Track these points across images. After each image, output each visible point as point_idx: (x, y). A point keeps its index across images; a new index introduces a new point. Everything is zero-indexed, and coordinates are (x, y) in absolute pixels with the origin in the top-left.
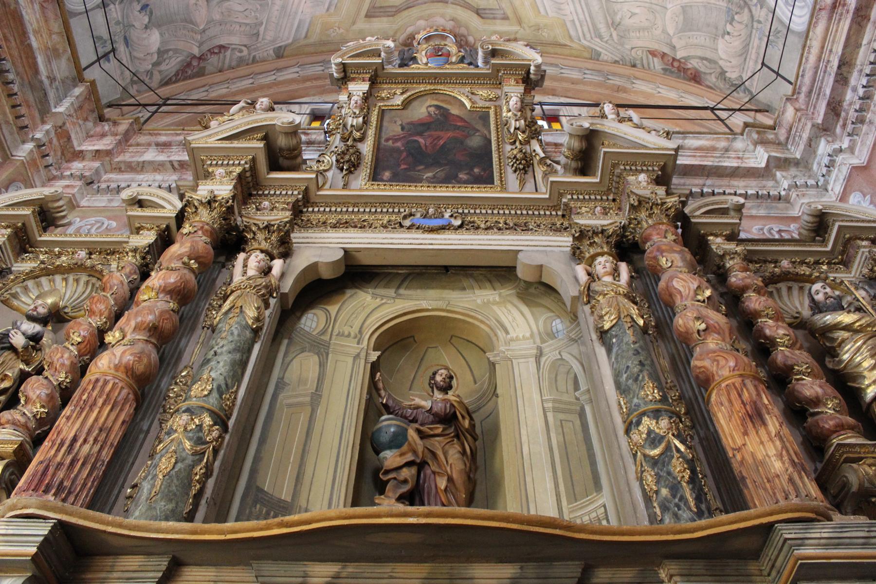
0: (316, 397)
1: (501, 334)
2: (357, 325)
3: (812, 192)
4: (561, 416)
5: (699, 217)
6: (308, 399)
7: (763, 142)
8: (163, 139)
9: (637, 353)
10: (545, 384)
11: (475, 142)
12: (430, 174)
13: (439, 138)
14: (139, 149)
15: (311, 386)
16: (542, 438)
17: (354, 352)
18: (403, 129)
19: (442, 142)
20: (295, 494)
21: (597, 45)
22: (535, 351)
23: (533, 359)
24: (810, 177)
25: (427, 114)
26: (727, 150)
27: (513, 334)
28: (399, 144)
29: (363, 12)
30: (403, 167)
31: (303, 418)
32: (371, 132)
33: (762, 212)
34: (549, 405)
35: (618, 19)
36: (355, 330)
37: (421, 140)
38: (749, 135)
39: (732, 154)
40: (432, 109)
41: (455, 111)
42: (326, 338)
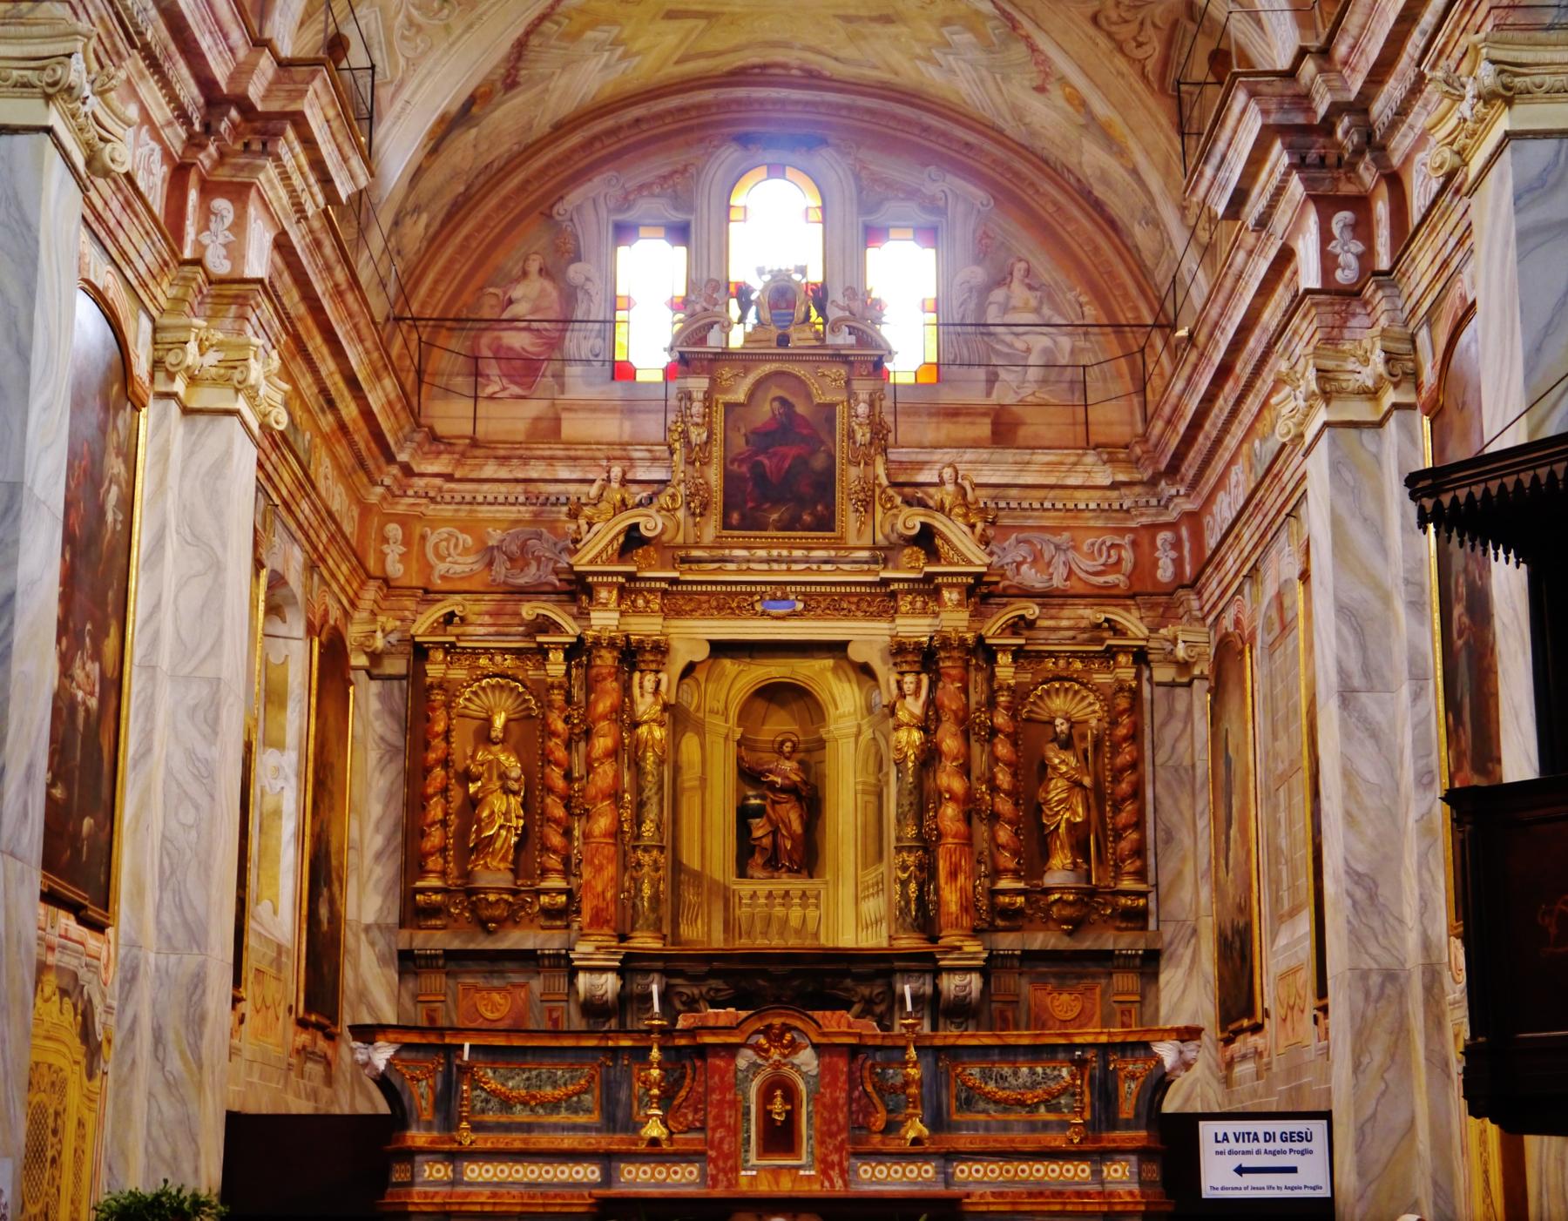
0: (703, 780)
1: (831, 709)
2: (723, 697)
3: (1153, 511)
4: (867, 798)
5: (992, 637)
6: (696, 783)
7: (1112, 460)
8: (502, 453)
9: (911, 793)
10: (859, 766)
11: (819, 462)
12: (775, 516)
13: (784, 458)
14: (477, 461)
15: (697, 770)
16: (851, 818)
17: (723, 731)
18: (747, 442)
19: (786, 465)
20: (703, 866)
21: (1000, 123)
22: (854, 730)
23: (852, 740)
24: (1154, 495)
25: (770, 415)
26: (1075, 464)
27: (841, 710)
28: (744, 469)
29: (675, 58)
30: (750, 505)
31: (697, 800)
32: (717, 451)
33: (1100, 524)
34: (860, 787)
35: (1028, 120)
36: (721, 706)
37: (766, 462)
38: (1099, 454)
39: (1080, 468)
40: (776, 404)
41: (801, 409)
42: (701, 715)
